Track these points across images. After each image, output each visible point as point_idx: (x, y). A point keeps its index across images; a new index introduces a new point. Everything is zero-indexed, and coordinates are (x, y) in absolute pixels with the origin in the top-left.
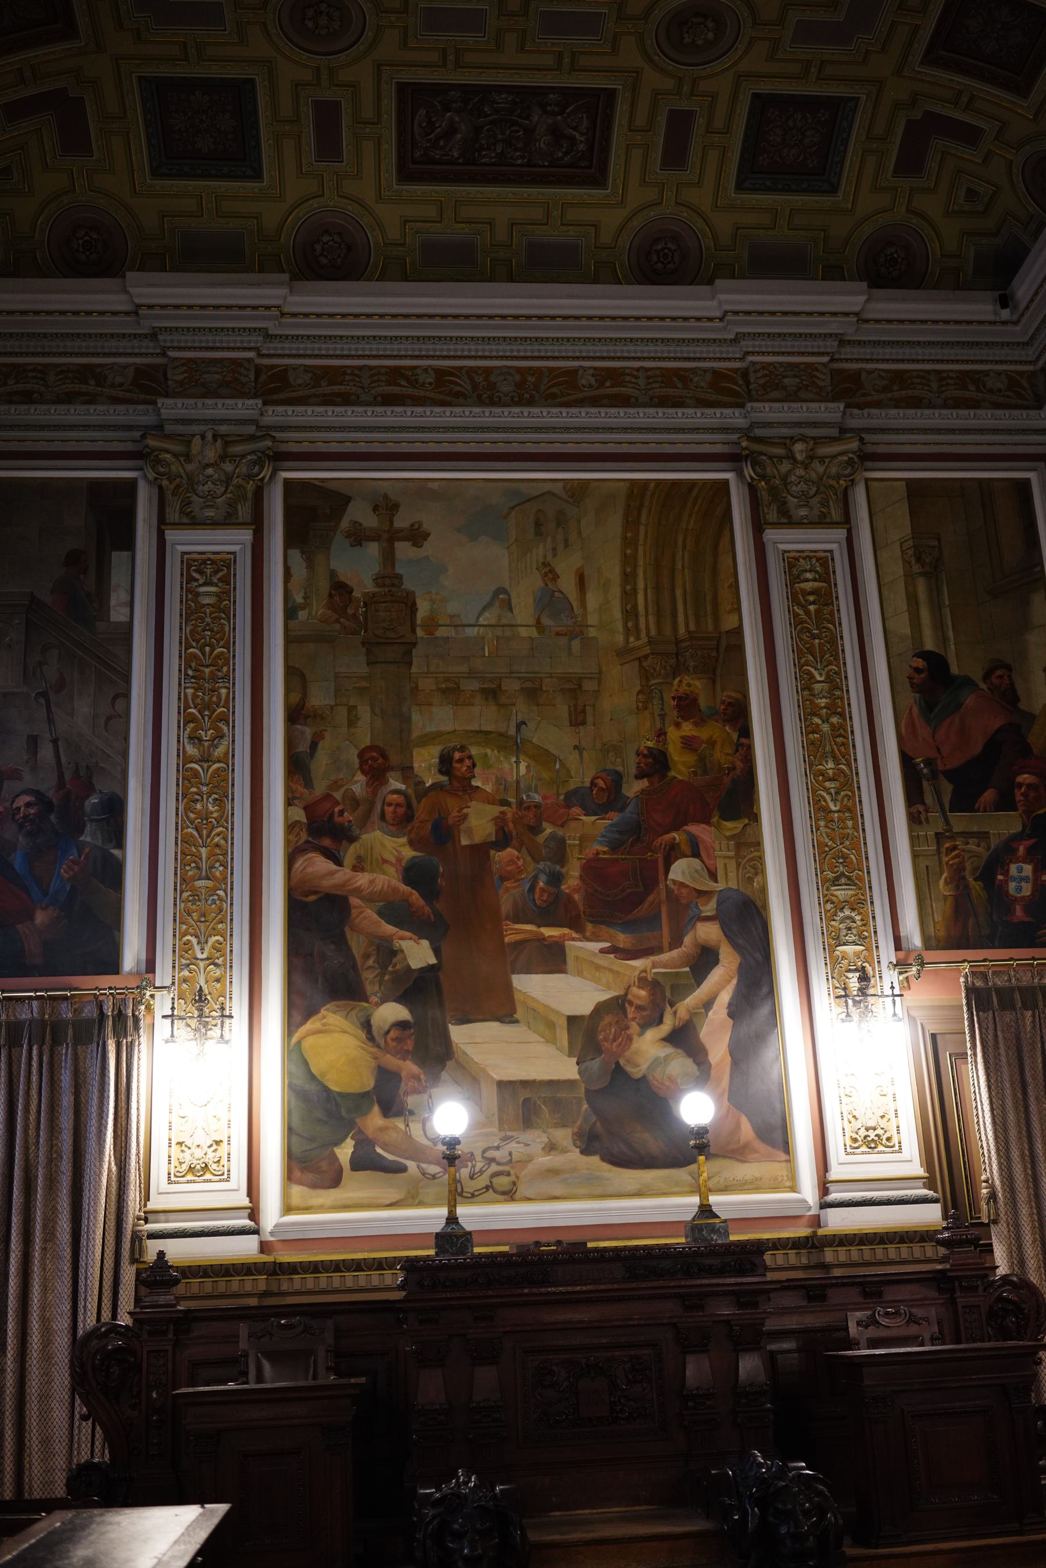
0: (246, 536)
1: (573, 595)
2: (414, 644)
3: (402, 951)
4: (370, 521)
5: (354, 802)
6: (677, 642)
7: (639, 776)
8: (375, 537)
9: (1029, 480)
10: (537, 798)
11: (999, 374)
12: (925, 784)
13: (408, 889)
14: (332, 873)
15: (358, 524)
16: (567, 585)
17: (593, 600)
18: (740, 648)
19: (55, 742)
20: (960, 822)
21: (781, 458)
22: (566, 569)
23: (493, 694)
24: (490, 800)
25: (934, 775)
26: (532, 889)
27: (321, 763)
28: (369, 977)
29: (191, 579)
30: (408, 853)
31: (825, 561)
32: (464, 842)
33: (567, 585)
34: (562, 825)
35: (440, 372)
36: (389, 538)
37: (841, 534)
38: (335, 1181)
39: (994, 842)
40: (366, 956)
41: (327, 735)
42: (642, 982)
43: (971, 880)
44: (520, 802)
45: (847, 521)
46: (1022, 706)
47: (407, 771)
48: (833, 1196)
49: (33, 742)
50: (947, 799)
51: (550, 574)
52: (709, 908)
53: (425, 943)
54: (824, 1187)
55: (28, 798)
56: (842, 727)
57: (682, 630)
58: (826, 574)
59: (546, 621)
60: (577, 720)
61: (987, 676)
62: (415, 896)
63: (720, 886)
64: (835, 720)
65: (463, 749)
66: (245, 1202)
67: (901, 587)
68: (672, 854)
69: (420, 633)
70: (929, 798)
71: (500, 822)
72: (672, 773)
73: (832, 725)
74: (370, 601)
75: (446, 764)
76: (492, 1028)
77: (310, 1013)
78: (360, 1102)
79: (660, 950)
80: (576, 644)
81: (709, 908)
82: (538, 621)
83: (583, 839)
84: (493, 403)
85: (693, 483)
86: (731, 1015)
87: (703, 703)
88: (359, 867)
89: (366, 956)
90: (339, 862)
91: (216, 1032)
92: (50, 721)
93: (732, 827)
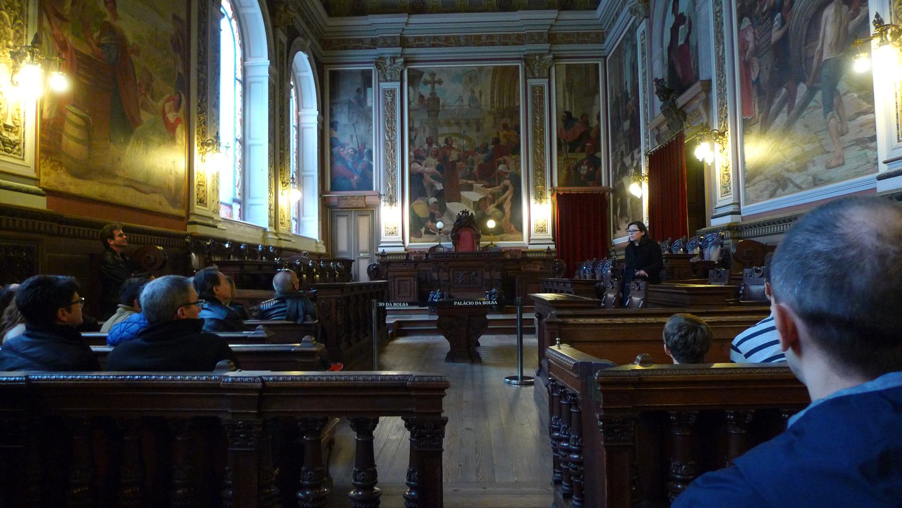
0: (399, 83)
1: (478, 98)
2: (439, 111)
3: (435, 186)
4: (429, 78)
5: (424, 151)
7: (492, 144)
8: (430, 83)
10: (468, 150)
11: (594, 32)
13: (436, 171)
15: (425, 79)
16: (477, 95)
17: (483, 99)
18: (519, 111)
19: (357, 136)
20: (570, 155)
22: (477, 90)
24: (457, 150)
27: (417, 141)
28: (428, 192)
29: (386, 95)
30: (437, 163)
31: (542, 87)
32: (450, 160)
33: (477, 95)
36: (433, 83)
38: (421, 236)
39: (578, 161)
40: (427, 187)
41: (419, 135)
42: (491, 193)
43: (571, 169)
46: (590, 125)
47: (437, 143)
49: (352, 136)
50: (568, 149)
51: (473, 92)
54: (529, 241)
58: (542, 92)
59: (471, 105)
60: (478, 130)
61: (582, 118)
64: (541, 130)
65: (450, 137)
66: (402, 240)
67: (562, 95)
68: (499, 163)
69: (441, 108)
70: (563, 150)
71: (459, 155)
72: (501, 143)
73: (540, 132)
74: (429, 100)
75: (446, 141)
76: (456, 204)
77: (415, 199)
78: (426, 219)
81: (507, 176)
82: (469, 105)
83: (479, 160)
84: (460, 45)
88: (426, 166)
89: (427, 187)
90: (421, 165)
93: (514, 157)
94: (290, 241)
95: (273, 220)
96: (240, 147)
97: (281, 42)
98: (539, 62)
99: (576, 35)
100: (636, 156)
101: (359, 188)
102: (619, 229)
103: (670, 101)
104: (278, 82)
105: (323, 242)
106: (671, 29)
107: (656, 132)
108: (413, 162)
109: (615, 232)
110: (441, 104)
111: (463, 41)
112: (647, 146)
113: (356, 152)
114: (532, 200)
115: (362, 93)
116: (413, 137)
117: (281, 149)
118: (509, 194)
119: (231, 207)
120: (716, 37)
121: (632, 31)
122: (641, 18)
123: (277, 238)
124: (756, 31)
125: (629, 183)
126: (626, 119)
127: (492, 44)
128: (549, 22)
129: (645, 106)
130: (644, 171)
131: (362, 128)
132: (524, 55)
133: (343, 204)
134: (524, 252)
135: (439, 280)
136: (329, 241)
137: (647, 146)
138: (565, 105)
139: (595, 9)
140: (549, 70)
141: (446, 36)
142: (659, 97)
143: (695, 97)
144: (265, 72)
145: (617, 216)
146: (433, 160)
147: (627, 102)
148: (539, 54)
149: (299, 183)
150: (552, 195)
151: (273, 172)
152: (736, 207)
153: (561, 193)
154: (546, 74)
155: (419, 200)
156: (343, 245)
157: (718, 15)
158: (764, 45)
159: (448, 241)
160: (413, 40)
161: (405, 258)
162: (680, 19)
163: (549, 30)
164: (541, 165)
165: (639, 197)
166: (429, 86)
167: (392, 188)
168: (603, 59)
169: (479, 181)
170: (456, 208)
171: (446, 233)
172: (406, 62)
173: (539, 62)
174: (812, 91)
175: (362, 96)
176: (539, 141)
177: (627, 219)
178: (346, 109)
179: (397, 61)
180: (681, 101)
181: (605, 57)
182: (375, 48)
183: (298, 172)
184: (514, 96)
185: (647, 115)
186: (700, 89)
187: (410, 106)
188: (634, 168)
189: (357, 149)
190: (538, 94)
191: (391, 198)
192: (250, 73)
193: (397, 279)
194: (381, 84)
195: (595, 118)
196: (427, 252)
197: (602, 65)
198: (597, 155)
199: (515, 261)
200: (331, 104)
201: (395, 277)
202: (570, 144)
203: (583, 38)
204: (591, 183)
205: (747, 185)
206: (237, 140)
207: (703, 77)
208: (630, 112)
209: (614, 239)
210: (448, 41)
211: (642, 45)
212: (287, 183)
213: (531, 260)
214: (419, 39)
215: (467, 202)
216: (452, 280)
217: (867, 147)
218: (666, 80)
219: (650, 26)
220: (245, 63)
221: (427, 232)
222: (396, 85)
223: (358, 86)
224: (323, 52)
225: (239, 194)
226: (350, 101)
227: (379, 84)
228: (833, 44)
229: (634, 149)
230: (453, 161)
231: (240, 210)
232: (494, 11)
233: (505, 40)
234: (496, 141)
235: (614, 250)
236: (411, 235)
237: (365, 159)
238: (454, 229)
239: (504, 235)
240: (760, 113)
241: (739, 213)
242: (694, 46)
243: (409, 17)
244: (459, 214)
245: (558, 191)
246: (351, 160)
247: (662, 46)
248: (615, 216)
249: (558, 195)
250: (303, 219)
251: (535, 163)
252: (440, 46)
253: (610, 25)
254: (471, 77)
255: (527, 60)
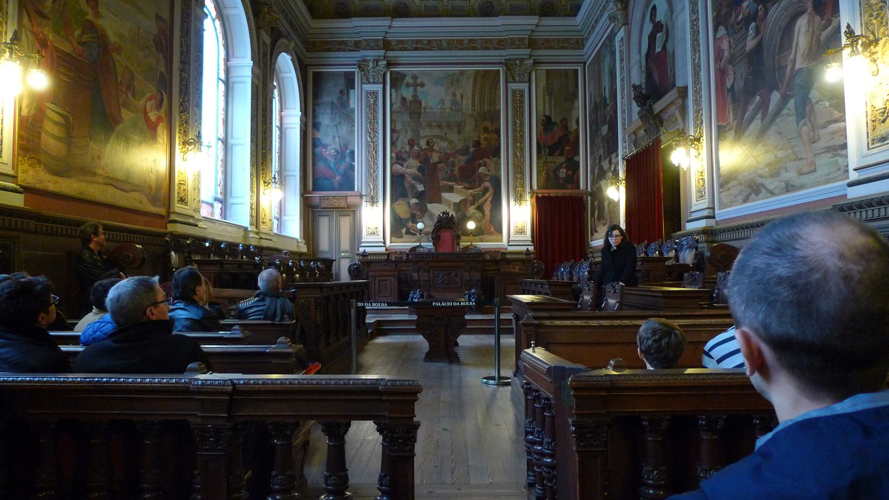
0: (381, 86)
4: (411, 81)
5: (407, 152)
6: (485, 113)
7: (473, 147)
8: (412, 85)
9: (577, 70)
10: (449, 152)
12: (542, 149)
13: (417, 173)
14: (401, 169)
16: (458, 98)
17: (464, 102)
18: (499, 115)
19: (339, 137)
20: (550, 159)
21: (513, 64)
23: (439, 126)
24: (438, 152)
25: (545, 147)
26: (447, 173)
28: (409, 193)
29: (369, 97)
30: (419, 164)
31: (522, 92)
32: (432, 162)
33: (458, 98)
34: (454, 158)
35: (429, 41)
36: (415, 85)
37: (528, 84)
38: (402, 237)
41: (401, 137)
44: (445, 153)
45: (530, 82)
46: (569, 129)
47: (419, 145)
48: (510, 244)
51: (455, 95)
52: (488, 179)
53: (422, 185)
54: (509, 242)
55: (334, 151)
56: (523, 135)
57: (486, 110)
58: (522, 96)
59: (453, 107)
60: (459, 133)
61: (561, 122)
62: (420, 175)
63: (491, 173)
64: (521, 133)
65: (432, 139)
66: (383, 240)
69: (422, 110)
70: (542, 152)
71: (440, 157)
73: (520, 135)
74: (411, 102)
75: (428, 143)
76: (437, 205)
77: (397, 200)
78: (407, 220)
79: (476, 188)
80: (460, 114)
81: (488, 179)
83: (459, 162)
84: (442, 49)
85: (491, 70)
86: (491, 203)
87: (490, 129)
88: (407, 168)
91: (376, 204)
92: (338, 132)
93: (494, 159)
94: (272, 240)
95: (254, 219)
96: (223, 146)
97: (264, 43)
98: (520, 67)
99: (556, 40)
100: (614, 160)
101: (341, 189)
102: (596, 232)
103: (647, 107)
104: (261, 82)
105: (304, 241)
106: (649, 36)
107: (633, 137)
108: (395, 163)
109: (592, 234)
110: (423, 106)
111: (445, 45)
112: (625, 150)
113: (338, 153)
114: (512, 202)
115: (344, 96)
116: (394, 139)
117: (263, 149)
118: (489, 196)
119: (212, 205)
120: (693, 45)
121: (611, 38)
122: (620, 25)
123: (258, 237)
124: (731, 41)
125: (607, 187)
126: (604, 124)
127: (475, 48)
128: (529, 28)
129: (623, 112)
130: (622, 175)
131: (344, 129)
132: (505, 60)
133: (325, 204)
134: (503, 253)
135: (419, 280)
136: (311, 242)
137: (625, 150)
138: (544, 108)
139: (575, 15)
140: (530, 74)
141: (427, 40)
142: (637, 102)
143: (671, 103)
144: (249, 73)
145: (594, 219)
146: (414, 161)
147: (605, 107)
148: (519, 59)
149: (281, 182)
150: (531, 197)
151: (254, 172)
152: (711, 211)
153: (540, 196)
154: (527, 80)
155: (400, 201)
156: (324, 245)
157: (695, 23)
158: (740, 53)
159: (429, 241)
160: (396, 43)
161: (386, 258)
162: (658, 27)
163: (530, 36)
164: (521, 168)
165: (616, 201)
166: (411, 89)
167: (374, 189)
168: (582, 65)
169: (459, 183)
170: (436, 209)
171: (427, 234)
172: (389, 65)
173: (520, 67)
174: (785, 99)
175: (345, 98)
176: (519, 144)
177: (604, 222)
178: (328, 110)
179: (380, 63)
180: (658, 107)
181: (585, 63)
182: (359, 51)
183: (280, 172)
184: (494, 101)
185: (625, 120)
186: (676, 95)
187: (393, 108)
188: (612, 172)
189: (339, 150)
190: (518, 98)
191: (372, 198)
192: (233, 73)
193: (377, 279)
194: (363, 86)
195: (574, 122)
196: (408, 252)
197: (581, 71)
198: (576, 158)
199: (495, 262)
200: (314, 105)
201: (375, 277)
202: (549, 147)
203: (564, 43)
204: (570, 186)
205: (721, 190)
206: (219, 139)
207: (680, 83)
208: (608, 117)
209: (591, 241)
210: (430, 45)
211: (621, 51)
212: (269, 183)
213: (509, 262)
214: (402, 42)
215: (448, 203)
216: (431, 278)
217: (838, 155)
218: (643, 86)
219: (629, 33)
220: (228, 63)
221: (408, 233)
222: (379, 87)
223: (341, 88)
224: (308, 55)
225: (221, 193)
226: (333, 102)
227: (361, 86)
228: (806, 53)
229: (612, 153)
230: (434, 163)
231: (221, 209)
232: (476, 16)
233: (487, 44)
234: (477, 144)
235: (591, 252)
236: (391, 236)
237: (347, 159)
238: (434, 230)
239: (484, 236)
240: (735, 119)
241: (714, 217)
242: (671, 51)
243: (392, 21)
244: (439, 215)
245: (537, 193)
246: (333, 160)
247: (640, 53)
248: (593, 219)
249: (537, 197)
250: (284, 218)
251: (515, 166)
252: (423, 49)
253: (590, 31)
254: (454, 80)
255: (508, 65)
